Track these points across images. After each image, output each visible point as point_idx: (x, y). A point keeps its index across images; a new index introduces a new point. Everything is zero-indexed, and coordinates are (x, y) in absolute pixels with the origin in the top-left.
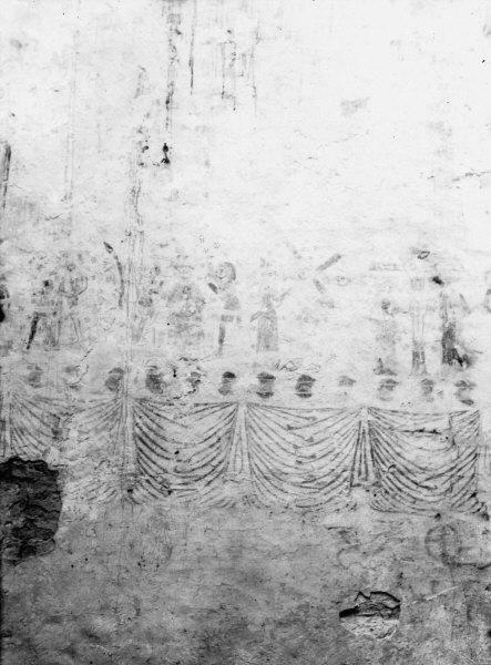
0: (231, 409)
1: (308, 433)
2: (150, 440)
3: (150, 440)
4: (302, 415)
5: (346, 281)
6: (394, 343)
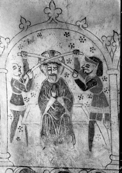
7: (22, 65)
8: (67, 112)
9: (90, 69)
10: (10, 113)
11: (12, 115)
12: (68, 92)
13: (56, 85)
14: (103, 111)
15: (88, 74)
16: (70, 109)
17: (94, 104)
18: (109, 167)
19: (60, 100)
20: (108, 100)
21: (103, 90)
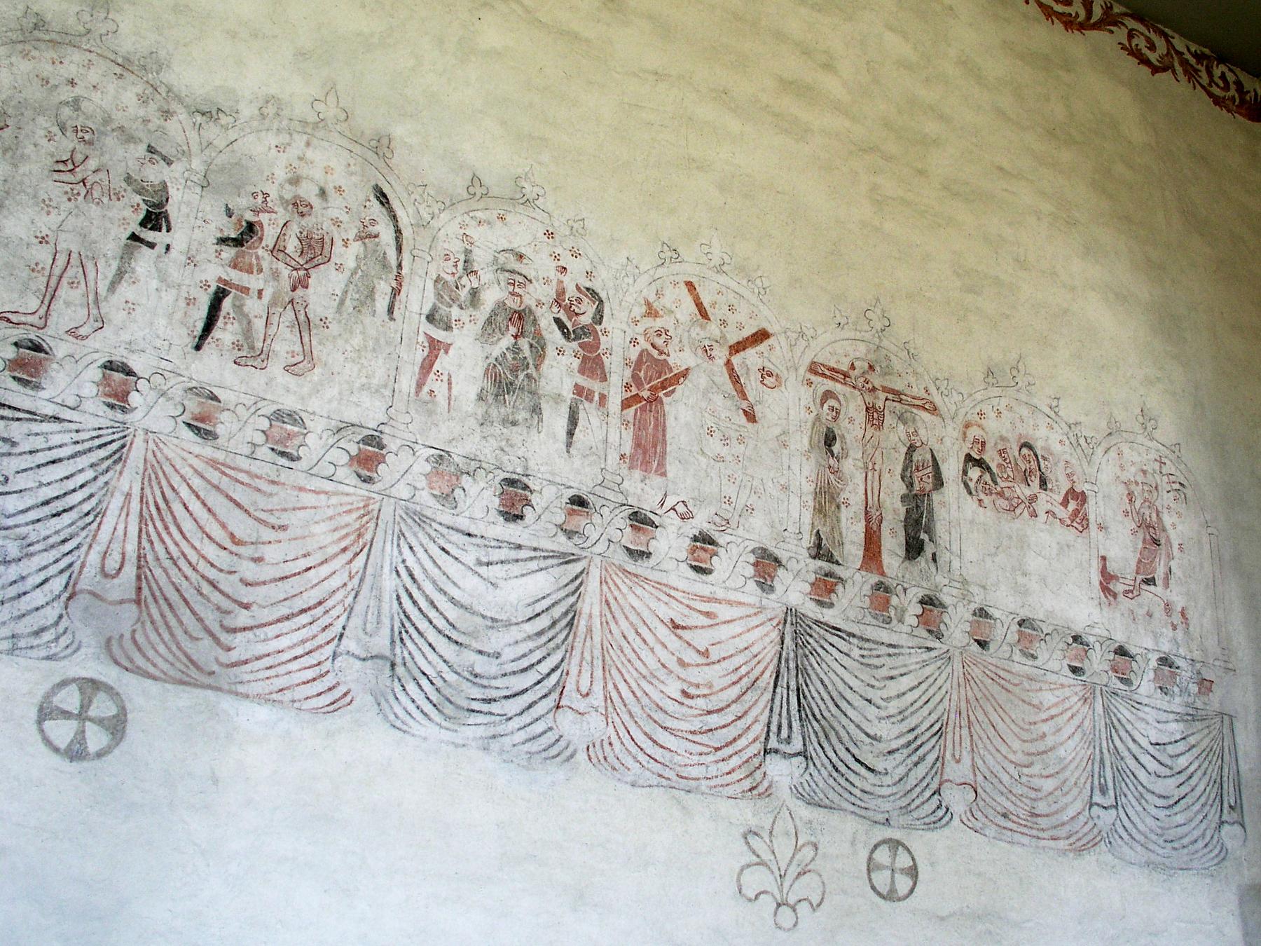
0: (578, 567)
1: (701, 639)
2: (427, 597)
3: (427, 597)
4: (692, 603)
5: (772, 379)
6: (838, 507)
7: (462, 258)
8: (532, 370)
10: (421, 338)
11: (426, 344)
12: (538, 336)
14: (596, 386)
15: (577, 314)
16: (537, 367)
17: (582, 371)
19: (524, 343)
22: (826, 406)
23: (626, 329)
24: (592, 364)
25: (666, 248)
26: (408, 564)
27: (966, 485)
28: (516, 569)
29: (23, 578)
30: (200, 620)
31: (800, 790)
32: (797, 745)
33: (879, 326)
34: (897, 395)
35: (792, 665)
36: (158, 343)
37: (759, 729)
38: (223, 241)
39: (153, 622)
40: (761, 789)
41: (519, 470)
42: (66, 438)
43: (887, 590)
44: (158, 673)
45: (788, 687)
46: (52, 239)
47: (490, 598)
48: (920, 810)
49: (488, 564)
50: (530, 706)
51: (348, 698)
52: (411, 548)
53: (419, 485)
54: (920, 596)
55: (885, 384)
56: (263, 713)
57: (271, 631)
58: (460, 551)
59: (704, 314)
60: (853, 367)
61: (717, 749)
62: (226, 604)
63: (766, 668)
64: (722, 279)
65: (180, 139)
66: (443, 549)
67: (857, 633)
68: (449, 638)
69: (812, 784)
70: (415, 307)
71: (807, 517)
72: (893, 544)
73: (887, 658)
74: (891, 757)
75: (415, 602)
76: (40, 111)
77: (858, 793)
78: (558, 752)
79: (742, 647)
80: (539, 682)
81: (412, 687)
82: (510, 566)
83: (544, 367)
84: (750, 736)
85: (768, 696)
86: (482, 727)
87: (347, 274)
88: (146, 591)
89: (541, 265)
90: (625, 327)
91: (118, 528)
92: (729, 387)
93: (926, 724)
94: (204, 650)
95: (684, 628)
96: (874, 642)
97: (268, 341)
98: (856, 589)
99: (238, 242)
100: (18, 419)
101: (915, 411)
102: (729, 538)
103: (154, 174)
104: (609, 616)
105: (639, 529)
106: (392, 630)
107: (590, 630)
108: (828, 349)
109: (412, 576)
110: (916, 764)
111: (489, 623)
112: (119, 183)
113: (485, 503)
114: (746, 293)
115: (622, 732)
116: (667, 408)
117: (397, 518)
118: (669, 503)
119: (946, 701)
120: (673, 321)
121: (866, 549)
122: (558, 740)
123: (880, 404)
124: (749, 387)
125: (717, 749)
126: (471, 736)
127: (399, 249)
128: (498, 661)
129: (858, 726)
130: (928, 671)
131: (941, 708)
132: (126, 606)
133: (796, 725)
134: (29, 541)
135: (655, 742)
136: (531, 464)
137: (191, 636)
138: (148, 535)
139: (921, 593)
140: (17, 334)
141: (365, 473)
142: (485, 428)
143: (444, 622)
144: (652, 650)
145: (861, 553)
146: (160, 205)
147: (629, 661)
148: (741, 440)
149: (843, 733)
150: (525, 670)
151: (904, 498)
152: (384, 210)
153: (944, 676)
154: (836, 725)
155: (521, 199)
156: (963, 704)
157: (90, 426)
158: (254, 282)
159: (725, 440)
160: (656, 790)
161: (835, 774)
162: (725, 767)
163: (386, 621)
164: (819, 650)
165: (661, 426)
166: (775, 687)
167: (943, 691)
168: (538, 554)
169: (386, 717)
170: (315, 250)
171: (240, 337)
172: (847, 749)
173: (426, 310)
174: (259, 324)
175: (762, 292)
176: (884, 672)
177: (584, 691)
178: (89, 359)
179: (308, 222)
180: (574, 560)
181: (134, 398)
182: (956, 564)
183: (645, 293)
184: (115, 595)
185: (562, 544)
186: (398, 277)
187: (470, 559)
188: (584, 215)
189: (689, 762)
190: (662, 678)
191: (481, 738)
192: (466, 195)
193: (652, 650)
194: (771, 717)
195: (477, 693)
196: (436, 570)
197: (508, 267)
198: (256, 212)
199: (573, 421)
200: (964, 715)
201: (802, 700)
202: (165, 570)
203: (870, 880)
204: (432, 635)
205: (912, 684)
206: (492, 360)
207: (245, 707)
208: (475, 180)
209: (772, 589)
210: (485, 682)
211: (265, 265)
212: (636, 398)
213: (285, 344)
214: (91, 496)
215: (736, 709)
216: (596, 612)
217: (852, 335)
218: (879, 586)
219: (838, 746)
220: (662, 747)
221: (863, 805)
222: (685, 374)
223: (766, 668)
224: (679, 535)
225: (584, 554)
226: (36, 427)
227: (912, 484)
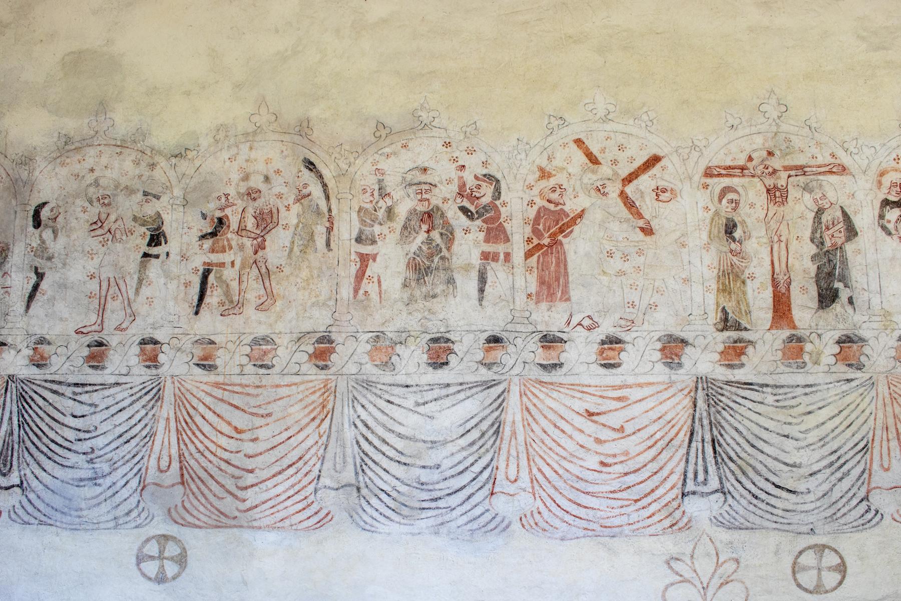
0: (500, 389)
1: (615, 420)
2: (379, 438)
3: (379, 438)
4: (605, 394)
5: (667, 195)
6: (744, 282)
7: (377, 187)
8: (445, 253)
9: (482, 191)
10: (353, 256)
11: (358, 260)
12: (446, 224)
13: (430, 215)
14: (501, 248)
15: (478, 198)
16: (448, 249)
17: (487, 240)
18: (509, 327)
19: (435, 235)
20: (509, 233)
21: (501, 220)
22: (724, 201)
23: (523, 196)
24: (496, 232)
25: (552, 119)
26: (362, 418)
27: (884, 228)
28: (447, 402)
29: (114, 483)
30: (223, 486)
31: (720, 519)
32: (714, 483)
33: (775, 115)
34: (801, 169)
35: (706, 422)
36: (171, 318)
37: (676, 478)
38: (203, 237)
39: (193, 494)
40: (681, 524)
41: (442, 330)
42: (126, 394)
43: (800, 340)
44: (201, 524)
45: (703, 441)
46: (97, 275)
47: (429, 427)
48: (847, 516)
49: (424, 404)
50: (469, 497)
51: (329, 517)
52: (363, 406)
53: (363, 361)
54: (836, 337)
55: (786, 163)
56: (272, 536)
57: (269, 484)
58: (401, 400)
59: (593, 160)
60: (750, 159)
61: (636, 501)
62: (238, 473)
63: (680, 430)
64: (609, 127)
65: (164, 179)
66: (389, 401)
67: (771, 382)
68: (399, 462)
69: (732, 512)
70: (345, 236)
71: (711, 299)
72: (803, 303)
73: (804, 397)
74: (811, 478)
75: (370, 443)
76: (77, 196)
77: (780, 513)
78: (498, 526)
79: (655, 417)
80: (474, 479)
81: (374, 501)
82: (442, 401)
83: (455, 247)
84: (668, 485)
85: (683, 451)
86: (433, 519)
87: (292, 229)
88: (186, 476)
89: (443, 171)
90: (521, 194)
91: (165, 442)
92: (625, 213)
93: (850, 444)
94: (228, 505)
95: (598, 414)
96: (788, 387)
97: (242, 294)
98: (767, 347)
99: (213, 234)
100: (96, 391)
101: (821, 177)
102: (634, 335)
103: (150, 210)
104: (530, 419)
105: (550, 348)
106: (355, 465)
107: (514, 433)
108: (722, 152)
109: (366, 426)
110: (840, 480)
111: (429, 445)
112: (130, 224)
113: (416, 360)
114: (634, 131)
115: (549, 502)
116: (566, 247)
117: (350, 388)
118: (575, 321)
119: (871, 422)
120: (565, 174)
121: (775, 310)
122: (494, 518)
123: (782, 182)
124: (645, 207)
125: (636, 501)
126: (425, 527)
127: (328, 198)
128: (439, 470)
129: (776, 459)
130: (848, 399)
131: (865, 428)
132: (176, 487)
133: (712, 469)
134: (113, 461)
135: (579, 505)
136: (452, 322)
137: (218, 498)
138: (184, 441)
139: (837, 335)
140: (87, 339)
141: (321, 363)
142: (410, 307)
143: (394, 452)
144: (570, 437)
145: (770, 315)
146: (159, 228)
147: (550, 449)
148: (640, 253)
149: (759, 467)
150: (462, 472)
151: (814, 258)
152: (312, 174)
153: (867, 400)
154: (752, 462)
155: (419, 125)
156: (891, 421)
157: (138, 383)
158: (227, 257)
159: (625, 258)
160: (583, 540)
161: (755, 501)
162: (647, 512)
163: (350, 460)
164: (732, 404)
165: (562, 263)
166: (690, 441)
167: (867, 413)
168: (464, 387)
169: (357, 524)
170: (267, 220)
171: (223, 298)
172: (767, 480)
173: (355, 234)
174: (234, 285)
175: (650, 124)
176: (802, 409)
177: (513, 479)
178: (131, 341)
179: (260, 203)
180: (495, 385)
181: (162, 358)
182: (876, 301)
183: (538, 162)
184: (168, 482)
185: (485, 374)
186: (330, 220)
187: (410, 403)
188: (476, 118)
189: (610, 514)
190: (581, 456)
191: (432, 526)
192: (373, 139)
193: (570, 437)
194: (686, 466)
195: (425, 496)
196: (385, 417)
197: (416, 181)
198: (222, 209)
199: (482, 279)
200: (892, 429)
201: (718, 448)
202: (196, 460)
203: (795, 580)
204: (385, 462)
205: (832, 414)
206: (411, 255)
207: (259, 535)
208: (380, 125)
209: (680, 365)
210: (431, 487)
211: (234, 243)
212: (539, 247)
213: (254, 291)
214: (146, 425)
215: (653, 467)
216: (518, 418)
217: (747, 131)
218: (791, 339)
219: (756, 479)
220: (586, 507)
221: (786, 521)
222: (580, 215)
223: (680, 430)
224: (587, 343)
225: (503, 378)
226: (107, 393)
227: (822, 243)
